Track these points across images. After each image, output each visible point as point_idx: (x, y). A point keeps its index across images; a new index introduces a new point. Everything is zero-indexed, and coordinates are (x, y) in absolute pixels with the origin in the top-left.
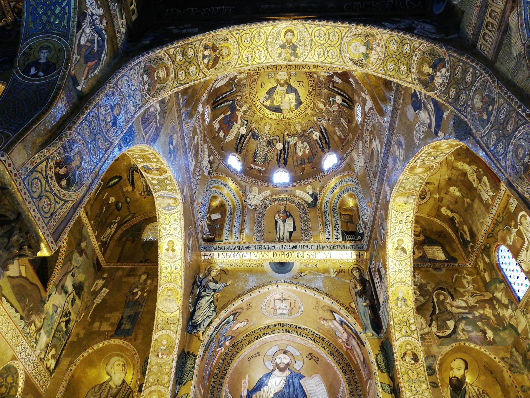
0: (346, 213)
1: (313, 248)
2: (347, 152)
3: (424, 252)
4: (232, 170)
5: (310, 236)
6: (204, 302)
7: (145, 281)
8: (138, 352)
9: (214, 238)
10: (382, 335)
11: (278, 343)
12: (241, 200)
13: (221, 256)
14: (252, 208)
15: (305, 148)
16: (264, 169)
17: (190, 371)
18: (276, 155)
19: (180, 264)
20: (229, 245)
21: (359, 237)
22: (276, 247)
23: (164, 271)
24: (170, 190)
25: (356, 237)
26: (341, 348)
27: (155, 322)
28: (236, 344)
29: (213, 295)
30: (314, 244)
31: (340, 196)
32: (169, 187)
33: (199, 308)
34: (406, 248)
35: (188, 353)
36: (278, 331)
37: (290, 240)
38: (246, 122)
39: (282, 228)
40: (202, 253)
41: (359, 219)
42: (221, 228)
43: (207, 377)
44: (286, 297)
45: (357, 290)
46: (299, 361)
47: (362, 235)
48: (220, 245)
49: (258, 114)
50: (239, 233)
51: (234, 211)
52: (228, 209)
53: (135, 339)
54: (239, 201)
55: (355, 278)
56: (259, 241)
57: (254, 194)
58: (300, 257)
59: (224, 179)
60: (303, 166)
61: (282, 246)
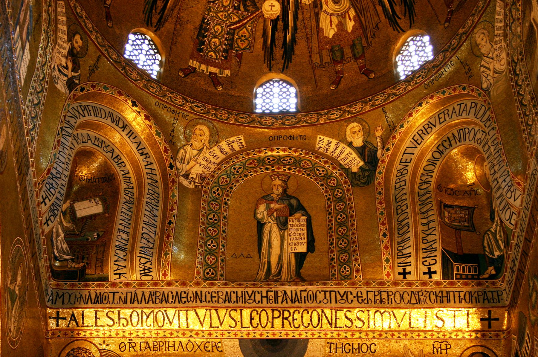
0: (457, 203)
2: (461, 31)
4: (134, 75)
5: (355, 265)
9: (83, 270)
12: (161, 161)
13: (104, 320)
14: (192, 186)
15: (343, 16)
16: (227, 73)
18: (259, 33)
20: (125, 290)
21: (491, 270)
25: (481, 271)
30: (364, 289)
31: (441, 153)
39: (276, 243)
40: (49, 311)
41: (492, 219)
48: (99, 290)
50: (155, 257)
51: (140, 193)
52: (123, 186)
54: (155, 166)
56: (211, 280)
57: (197, 145)
58: (326, 326)
59: (113, 102)
60: (339, 67)
61: (276, 293)
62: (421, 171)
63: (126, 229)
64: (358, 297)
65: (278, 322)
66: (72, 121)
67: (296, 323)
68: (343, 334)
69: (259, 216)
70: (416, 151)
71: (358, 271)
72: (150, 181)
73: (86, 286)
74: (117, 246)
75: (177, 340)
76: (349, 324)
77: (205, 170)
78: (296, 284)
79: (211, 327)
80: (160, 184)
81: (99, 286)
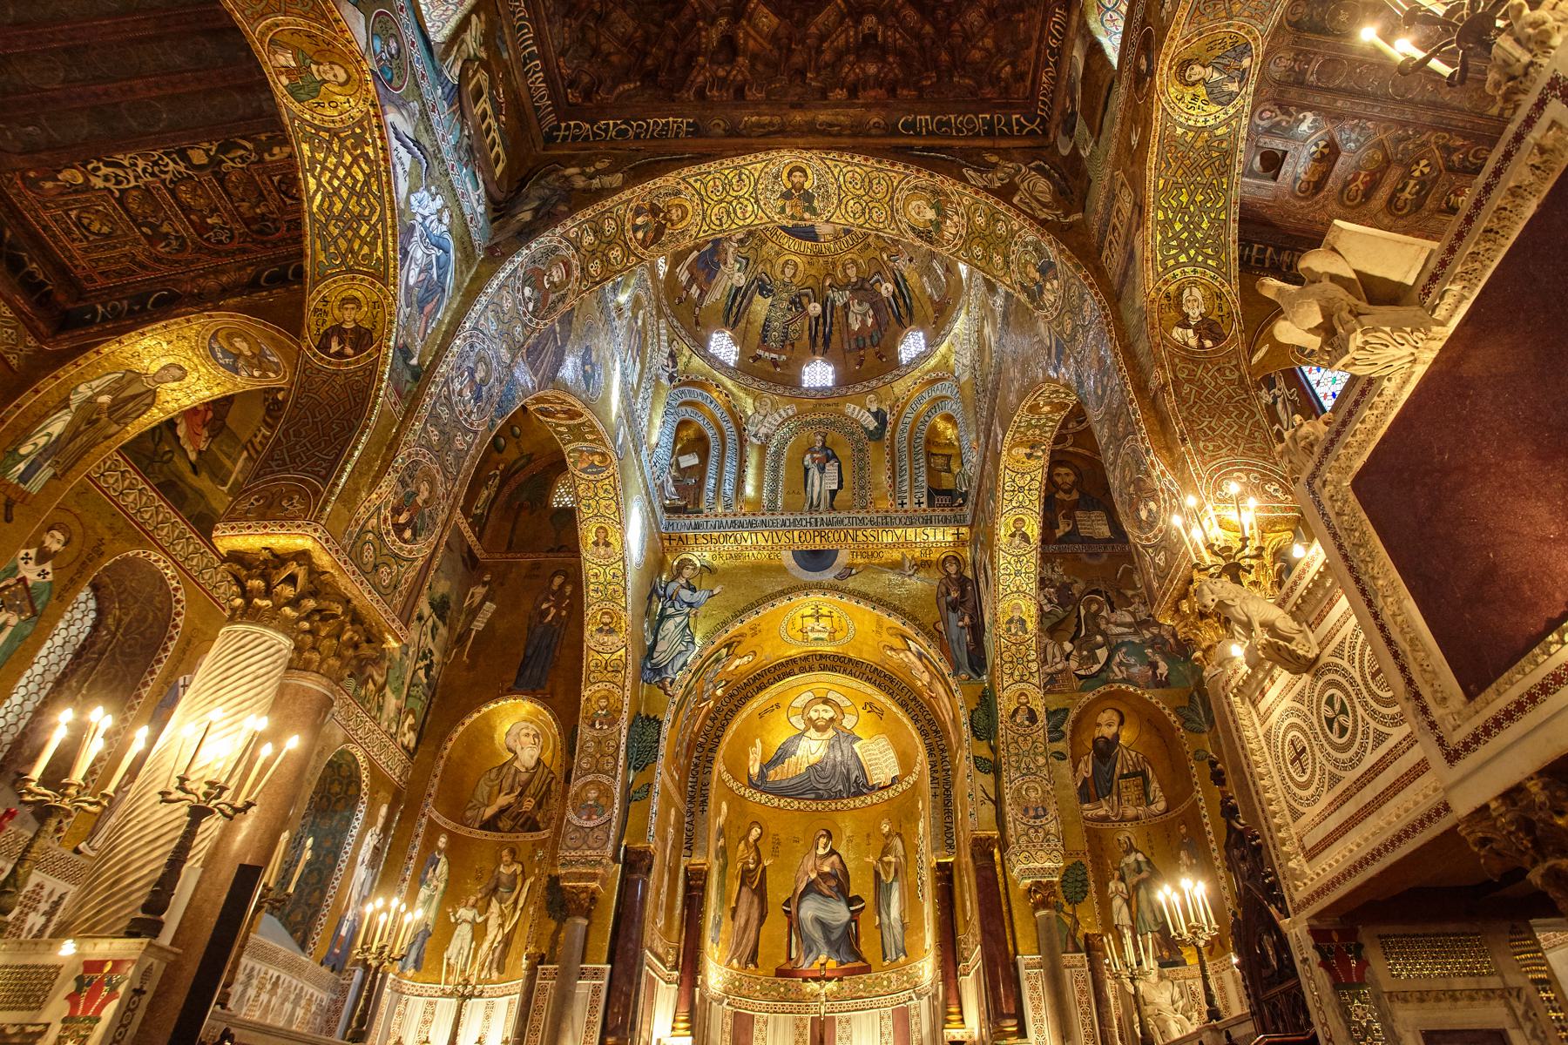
11: (812, 686)
15: (865, 315)
16: (784, 357)
18: (806, 327)
21: (960, 501)
24: (591, 441)
25: (953, 501)
26: (921, 696)
29: (688, 615)
30: (875, 515)
32: (590, 437)
35: (647, 717)
37: (832, 508)
38: (744, 262)
39: (817, 483)
43: (684, 752)
44: (824, 611)
45: (949, 599)
47: (965, 496)
49: (770, 244)
55: (949, 575)
56: (773, 511)
58: (850, 541)
60: (862, 353)
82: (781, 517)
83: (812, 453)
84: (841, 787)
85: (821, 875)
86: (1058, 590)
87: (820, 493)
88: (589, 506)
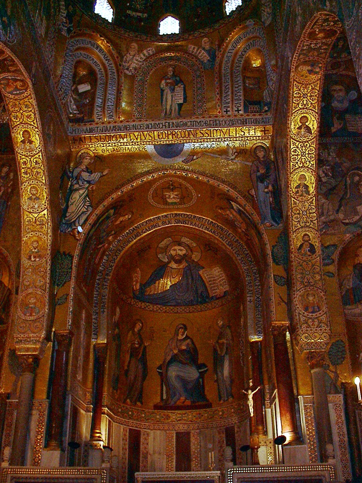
1: (208, 125)
3: (345, 124)
6: (77, 197)
7: (8, 174)
8: (10, 254)
9: (83, 117)
10: (281, 225)
14: (130, 74)
16: (146, 15)
17: (67, 272)
19: (41, 157)
20: (102, 126)
21: (266, 108)
22: (161, 126)
23: (23, 167)
24: (14, 72)
27: (22, 223)
28: (122, 239)
30: (208, 119)
31: (245, 52)
32: (13, 69)
33: (72, 204)
34: (312, 128)
35: (64, 253)
36: (169, 222)
37: (179, 116)
39: (169, 98)
42: (92, 104)
45: (259, 174)
46: (196, 252)
47: (269, 104)
50: (114, 109)
52: (99, 76)
53: (5, 241)
54: (113, 65)
62: (236, 61)
63: (101, 97)
64: (206, 123)
65: (170, 137)
66: (71, 48)
67: (179, 136)
68: (200, 140)
69: (162, 86)
70: (234, 51)
71: (206, 111)
72: (111, 73)
73: (85, 125)
74: (97, 106)
75: (126, 146)
76: (202, 136)
77: (137, 66)
78: (178, 119)
79: (141, 140)
80: (115, 74)
81: (91, 124)
82: (146, 123)
83: (166, 79)
84: (192, 298)
85: (181, 351)
86: (332, 169)
87: (171, 105)
88: (16, 117)
